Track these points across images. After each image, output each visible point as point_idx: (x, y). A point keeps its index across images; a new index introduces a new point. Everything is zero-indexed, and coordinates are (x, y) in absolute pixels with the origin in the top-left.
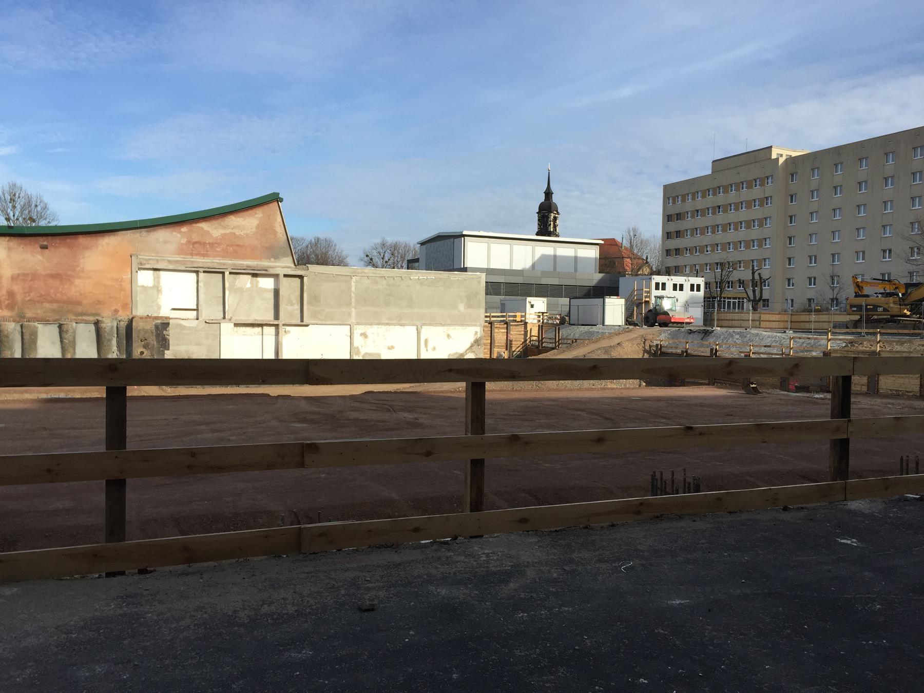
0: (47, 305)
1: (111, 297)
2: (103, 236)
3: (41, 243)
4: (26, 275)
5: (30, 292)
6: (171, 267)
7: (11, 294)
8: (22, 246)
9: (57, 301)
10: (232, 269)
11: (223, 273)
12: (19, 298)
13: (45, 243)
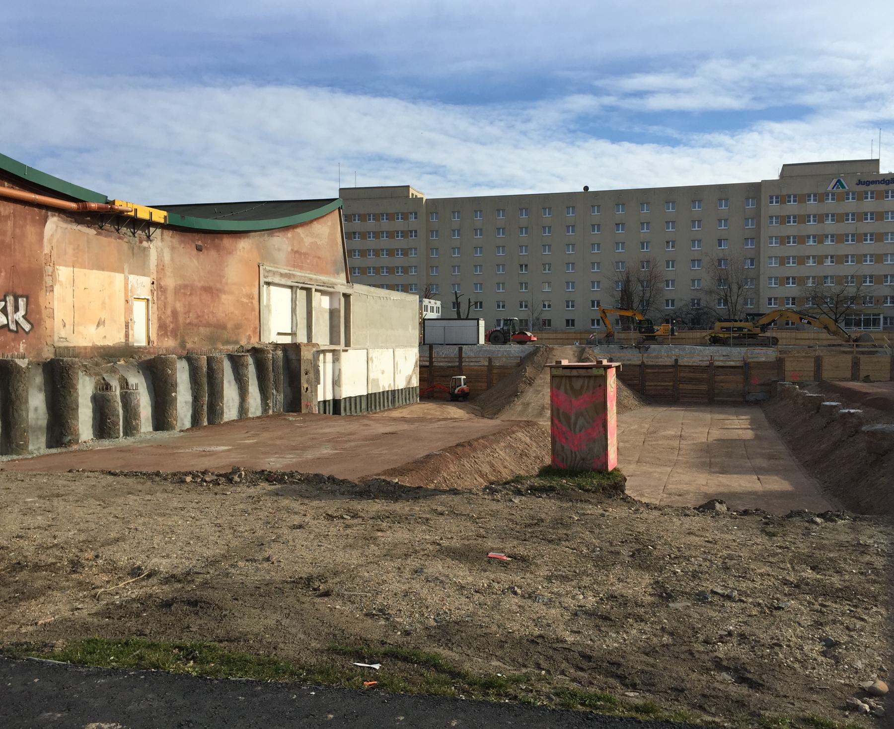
0: (202, 330)
1: (245, 319)
2: (240, 238)
3: (197, 243)
4: (185, 286)
5: (189, 312)
6: (283, 281)
7: (175, 313)
8: (182, 246)
9: (208, 325)
10: (317, 285)
11: (308, 291)
12: (181, 319)
13: (199, 243)
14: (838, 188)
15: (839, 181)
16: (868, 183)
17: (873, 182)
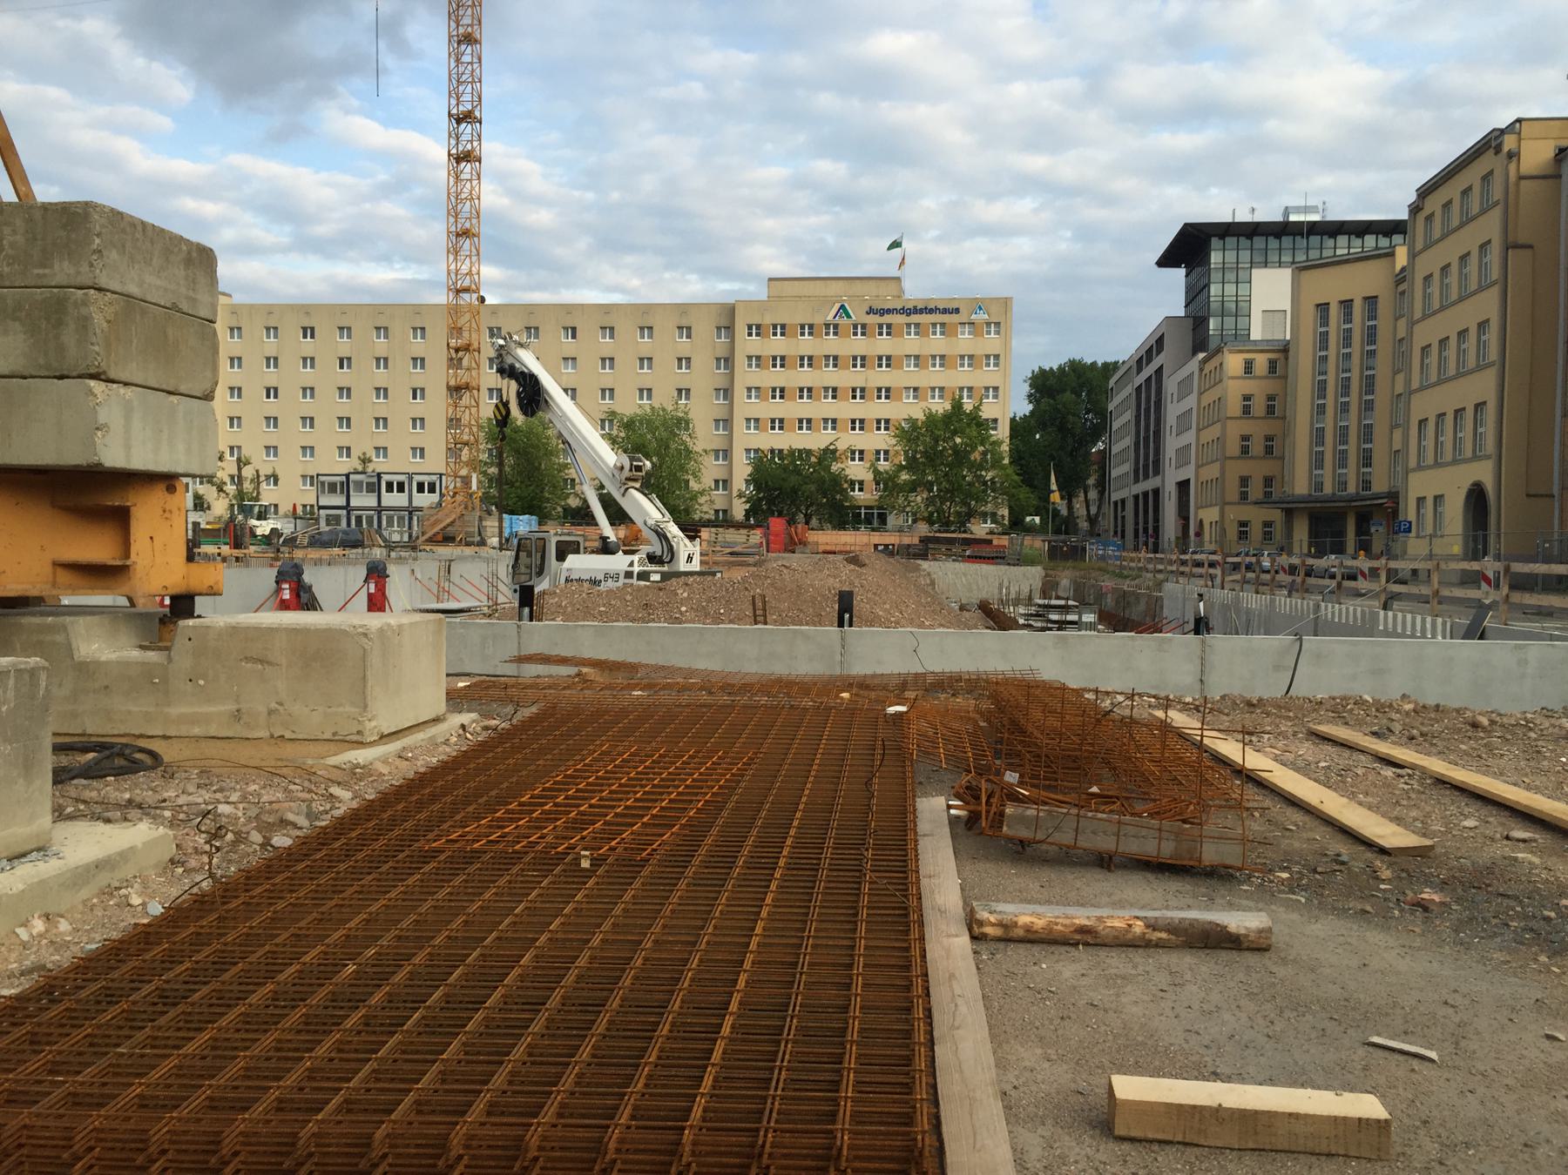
14: (841, 317)
15: (842, 307)
16: (883, 312)
17: (889, 311)
